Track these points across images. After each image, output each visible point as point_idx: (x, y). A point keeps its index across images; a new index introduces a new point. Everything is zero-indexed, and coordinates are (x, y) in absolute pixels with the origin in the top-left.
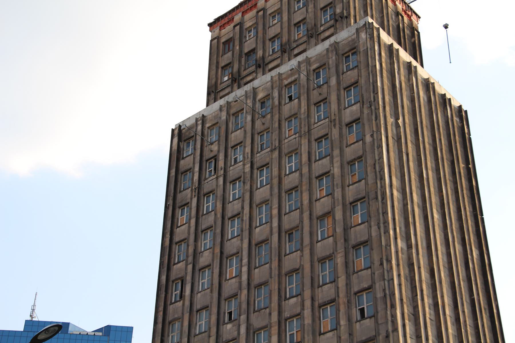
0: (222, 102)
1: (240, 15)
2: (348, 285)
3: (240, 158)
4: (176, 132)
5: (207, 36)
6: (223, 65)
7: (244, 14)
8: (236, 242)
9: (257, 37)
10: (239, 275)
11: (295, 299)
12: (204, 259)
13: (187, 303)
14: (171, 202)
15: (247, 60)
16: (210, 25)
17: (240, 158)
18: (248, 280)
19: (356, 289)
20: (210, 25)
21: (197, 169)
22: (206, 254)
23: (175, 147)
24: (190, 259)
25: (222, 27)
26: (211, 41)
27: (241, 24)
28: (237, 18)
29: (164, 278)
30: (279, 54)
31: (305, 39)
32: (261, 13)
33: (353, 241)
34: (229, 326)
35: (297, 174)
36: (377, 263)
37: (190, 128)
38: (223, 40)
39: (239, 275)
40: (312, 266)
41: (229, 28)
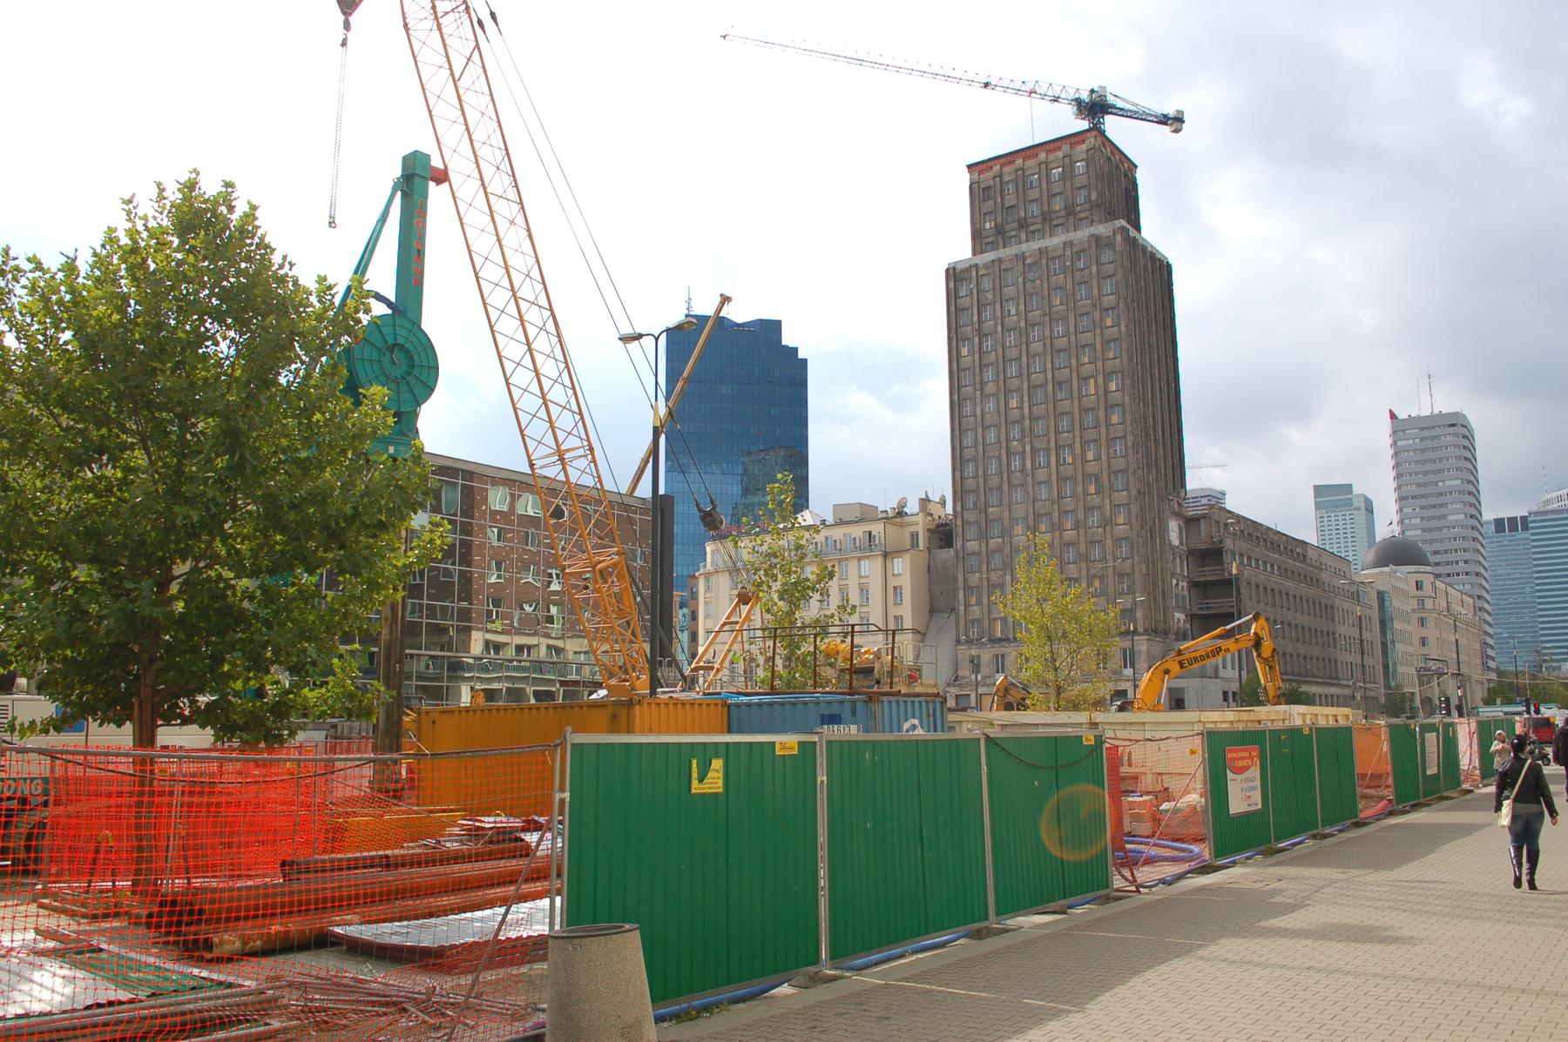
0: (989, 256)
1: (999, 167)
2: (1107, 433)
3: (1013, 311)
4: (951, 272)
5: (965, 179)
6: (985, 211)
7: (1002, 166)
8: (1015, 382)
9: (1017, 192)
10: (1021, 408)
11: (1066, 434)
12: (990, 388)
13: (979, 419)
14: (953, 334)
15: (1007, 214)
16: (969, 167)
17: (1013, 311)
18: (1030, 413)
19: (1112, 436)
20: (969, 167)
21: (975, 311)
22: (990, 384)
23: (952, 286)
24: (978, 386)
25: (980, 173)
26: (971, 187)
27: (1001, 176)
28: (997, 168)
29: (956, 397)
30: (1039, 220)
31: (1063, 213)
32: (1020, 172)
33: (1110, 403)
34: (1015, 443)
35: (1065, 339)
36: (1128, 423)
37: (963, 271)
38: (982, 186)
39: (1021, 408)
40: (1080, 415)
41: (990, 174)
